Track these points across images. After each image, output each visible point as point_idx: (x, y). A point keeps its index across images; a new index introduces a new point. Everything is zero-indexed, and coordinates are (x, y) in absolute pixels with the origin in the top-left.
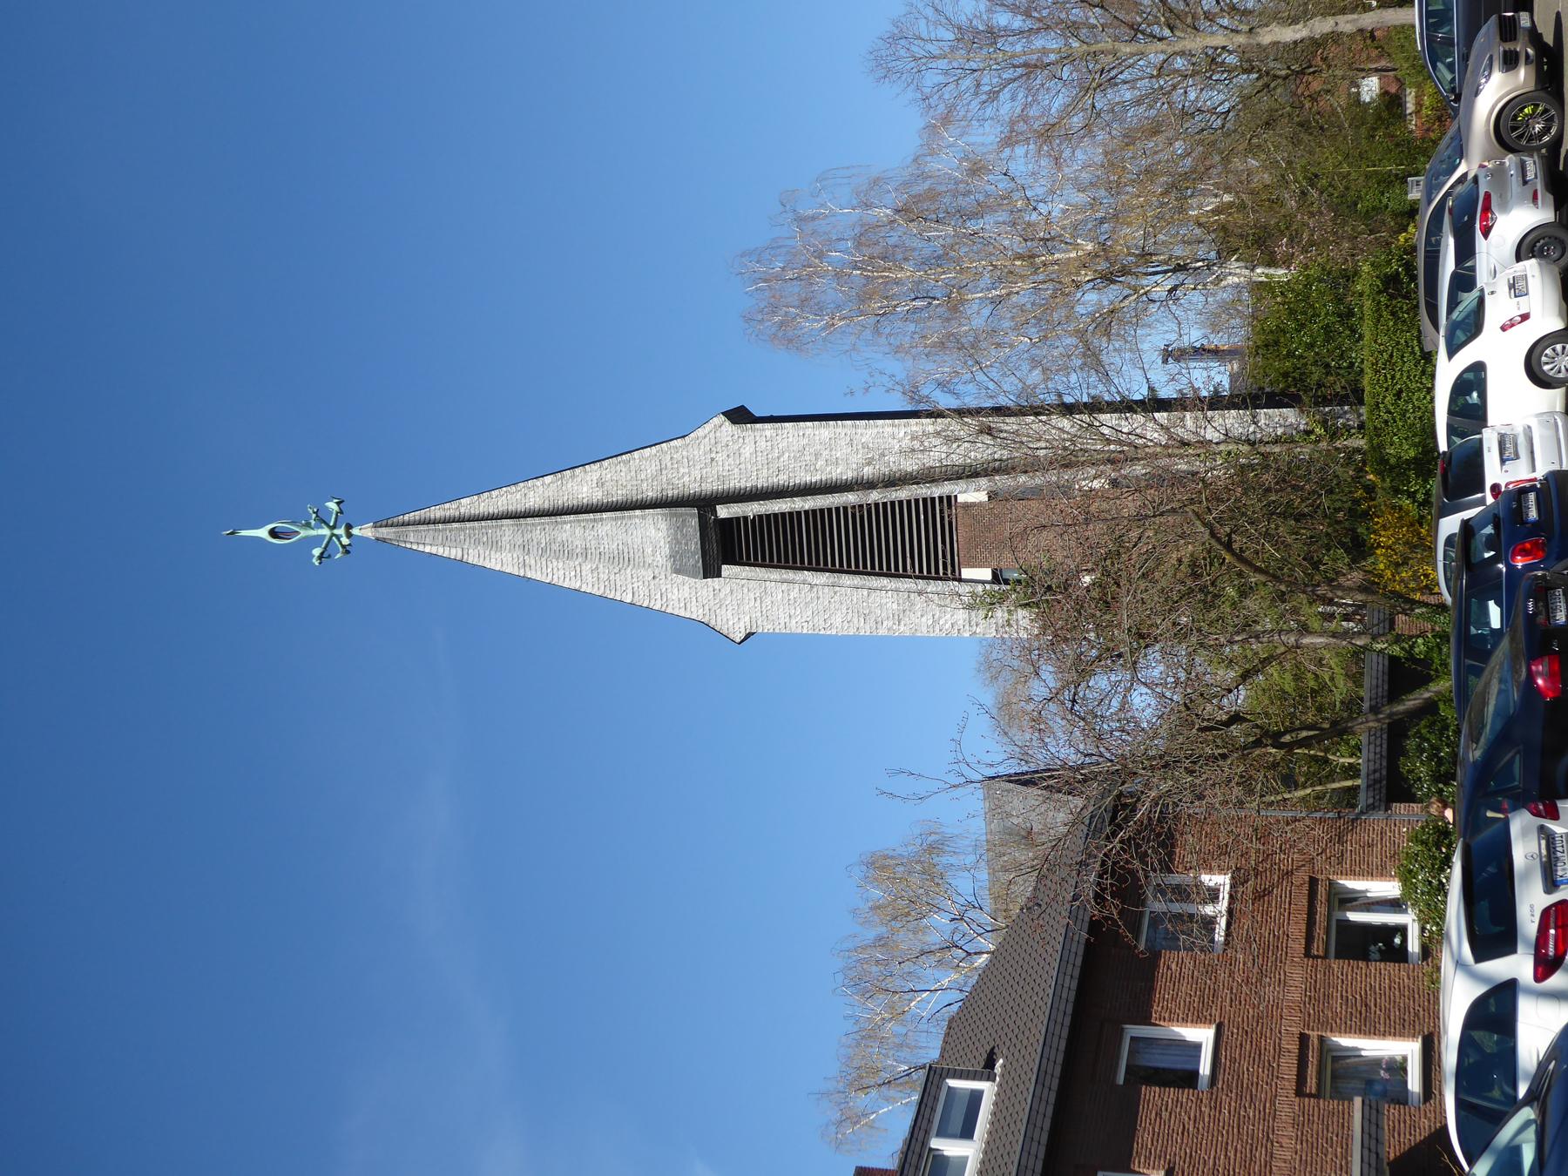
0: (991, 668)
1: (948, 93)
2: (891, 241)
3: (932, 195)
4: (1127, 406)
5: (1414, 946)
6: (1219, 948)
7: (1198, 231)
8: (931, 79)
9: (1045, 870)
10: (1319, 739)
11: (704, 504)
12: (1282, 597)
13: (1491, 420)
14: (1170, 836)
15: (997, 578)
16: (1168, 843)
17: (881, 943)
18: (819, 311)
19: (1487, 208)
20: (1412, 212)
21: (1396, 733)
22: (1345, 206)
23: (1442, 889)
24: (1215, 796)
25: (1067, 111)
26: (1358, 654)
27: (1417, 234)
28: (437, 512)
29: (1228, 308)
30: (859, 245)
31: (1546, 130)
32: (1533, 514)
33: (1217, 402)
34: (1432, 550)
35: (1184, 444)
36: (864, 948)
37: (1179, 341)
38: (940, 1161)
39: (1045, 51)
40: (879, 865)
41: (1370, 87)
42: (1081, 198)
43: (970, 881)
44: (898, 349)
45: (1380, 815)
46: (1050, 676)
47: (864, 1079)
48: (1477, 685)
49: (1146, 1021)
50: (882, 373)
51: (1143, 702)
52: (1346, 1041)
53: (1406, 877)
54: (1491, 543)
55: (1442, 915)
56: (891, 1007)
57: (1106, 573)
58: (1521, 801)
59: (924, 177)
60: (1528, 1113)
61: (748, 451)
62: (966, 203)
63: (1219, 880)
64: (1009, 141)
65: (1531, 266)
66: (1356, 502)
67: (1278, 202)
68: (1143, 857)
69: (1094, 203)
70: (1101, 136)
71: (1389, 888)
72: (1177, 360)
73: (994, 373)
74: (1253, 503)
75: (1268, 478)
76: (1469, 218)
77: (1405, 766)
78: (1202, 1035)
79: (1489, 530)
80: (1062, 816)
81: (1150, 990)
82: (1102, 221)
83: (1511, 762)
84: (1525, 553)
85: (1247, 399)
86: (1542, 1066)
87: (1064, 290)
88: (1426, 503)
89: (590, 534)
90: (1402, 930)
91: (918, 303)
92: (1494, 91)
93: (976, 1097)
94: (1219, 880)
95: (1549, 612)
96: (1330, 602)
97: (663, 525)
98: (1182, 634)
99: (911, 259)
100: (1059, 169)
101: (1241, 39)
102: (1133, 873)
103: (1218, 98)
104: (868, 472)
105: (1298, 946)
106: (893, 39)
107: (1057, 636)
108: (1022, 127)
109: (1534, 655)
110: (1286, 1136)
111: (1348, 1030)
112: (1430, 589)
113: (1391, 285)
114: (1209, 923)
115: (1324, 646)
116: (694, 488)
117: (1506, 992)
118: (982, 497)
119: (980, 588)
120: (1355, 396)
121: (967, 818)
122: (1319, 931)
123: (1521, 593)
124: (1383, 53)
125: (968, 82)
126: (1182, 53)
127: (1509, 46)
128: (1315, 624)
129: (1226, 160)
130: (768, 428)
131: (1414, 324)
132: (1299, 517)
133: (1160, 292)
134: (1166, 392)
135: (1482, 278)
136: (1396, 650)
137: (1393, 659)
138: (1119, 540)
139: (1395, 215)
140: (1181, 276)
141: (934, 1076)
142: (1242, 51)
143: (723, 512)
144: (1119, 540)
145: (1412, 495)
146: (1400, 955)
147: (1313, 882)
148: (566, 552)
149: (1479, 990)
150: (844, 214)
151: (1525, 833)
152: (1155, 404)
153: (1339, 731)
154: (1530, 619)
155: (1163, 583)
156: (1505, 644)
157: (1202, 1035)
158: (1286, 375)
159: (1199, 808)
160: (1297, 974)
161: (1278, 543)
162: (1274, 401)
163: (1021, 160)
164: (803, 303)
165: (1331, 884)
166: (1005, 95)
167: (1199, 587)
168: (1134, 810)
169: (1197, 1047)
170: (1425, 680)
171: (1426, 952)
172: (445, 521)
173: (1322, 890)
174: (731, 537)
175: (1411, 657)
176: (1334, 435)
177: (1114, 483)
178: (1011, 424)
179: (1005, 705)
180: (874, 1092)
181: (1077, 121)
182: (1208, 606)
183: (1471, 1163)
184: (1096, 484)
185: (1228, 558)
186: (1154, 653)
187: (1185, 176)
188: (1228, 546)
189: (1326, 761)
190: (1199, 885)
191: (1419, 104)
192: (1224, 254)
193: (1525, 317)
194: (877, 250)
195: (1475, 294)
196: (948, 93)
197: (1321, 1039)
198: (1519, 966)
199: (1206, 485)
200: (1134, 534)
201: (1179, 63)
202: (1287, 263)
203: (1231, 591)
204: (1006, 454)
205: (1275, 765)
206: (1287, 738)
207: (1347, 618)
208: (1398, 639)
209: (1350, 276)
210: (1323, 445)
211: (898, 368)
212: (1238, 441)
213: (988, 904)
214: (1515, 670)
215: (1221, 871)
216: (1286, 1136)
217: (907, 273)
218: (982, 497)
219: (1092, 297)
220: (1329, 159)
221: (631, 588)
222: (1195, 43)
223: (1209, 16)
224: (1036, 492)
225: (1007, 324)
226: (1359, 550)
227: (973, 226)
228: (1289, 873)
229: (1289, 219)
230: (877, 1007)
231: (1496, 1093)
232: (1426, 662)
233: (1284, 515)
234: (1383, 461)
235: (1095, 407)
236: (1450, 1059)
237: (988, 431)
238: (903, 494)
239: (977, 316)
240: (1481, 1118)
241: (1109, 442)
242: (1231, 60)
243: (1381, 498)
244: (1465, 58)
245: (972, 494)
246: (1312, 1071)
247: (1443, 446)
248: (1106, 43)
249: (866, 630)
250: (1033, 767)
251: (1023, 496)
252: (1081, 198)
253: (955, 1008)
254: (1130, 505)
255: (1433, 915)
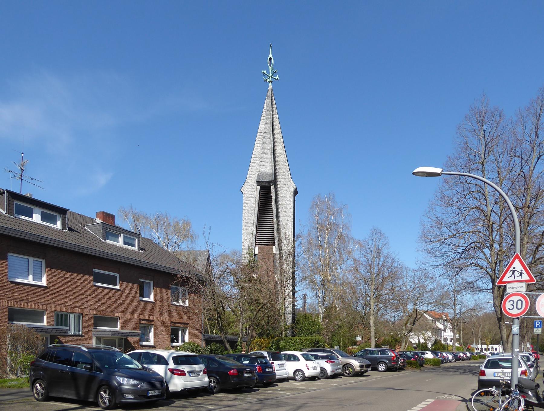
0: (234, 253)
1: (367, 246)
2: (334, 232)
3: (344, 242)
4: (294, 286)
5: (174, 344)
6: (172, 303)
7: (331, 302)
8: (370, 242)
9: (188, 264)
10: (219, 326)
11: (275, 182)
12: (250, 319)
13: (287, 362)
14: (197, 293)
15: (255, 255)
16: (195, 293)
17: (169, 224)
18: (320, 214)
19: (331, 362)
20: (332, 347)
21: (221, 342)
22: (334, 333)
23: (187, 350)
24: (206, 303)
25: (360, 273)
26: (238, 335)
27: (327, 348)
28: (275, 108)
29: (314, 308)
30: (334, 224)
31: (347, 373)
32: (267, 370)
33: (294, 306)
34: (260, 350)
35: (285, 299)
36: (167, 219)
37: (307, 298)
38: (118, 236)
39: (374, 269)
40: (187, 224)
41: (359, 339)
42: (340, 277)
43: (185, 246)
44: (309, 233)
45: (203, 338)
46: (233, 267)
47: (136, 219)
48: (231, 359)
49: (154, 286)
50: (304, 229)
51: (227, 288)
52: (153, 330)
53: (189, 343)
54: (261, 362)
55: (182, 350)
56: (154, 226)
57: (256, 280)
58: (207, 367)
59: (349, 240)
60: (140, 366)
61: (287, 194)
62: (342, 250)
63: (187, 304)
64: (355, 260)
65: (319, 370)
66: (271, 335)
67: (336, 319)
68: (192, 287)
69: (339, 279)
70: (354, 281)
71: (187, 340)
72: (303, 297)
73: (302, 255)
74: (271, 313)
75: (277, 316)
76: (330, 358)
77: (214, 344)
78: (152, 299)
79: (264, 361)
80: (200, 268)
81: (162, 288)
82: (335, 281)
83: (214, 365)
84: (259, 369)
85: (294, 313)
86: (151, 370)
87: (320, 272)
88: (270, 349)
89: (268, 151)
90: (178, 342)
91: (320, 238)
92: (356, 363)
93: (134, 246)
94: (187, 304)
95: (246, 373)
96: (249, 329)
97: (270, 171)
98: (242, 297)
99: (330, 235)
100: (348, 271)
101: (372, 312)
102: (188, 284)
103: (360, 306)
104: (281, 224)
105: (173, 320)
106: (380, 234)
107: (242, 269)
108: (358, 263)
109: (237, 370)
110: (131, 316)
111: (155, 330)
112: (252, 349)
113: (317, 343)
114: (177, 301)
115: (240, 328)
116: (279, 180)
117: (166, 363)
118: (274, 252)
119: (253, 251)
120: (294, 335)
121: (200, 246)
122: (177, 325)
123: (251, 368)
124: (366, 341)
125: (369, 251)
126: (370, 299)
127: (364, 366)
128: (244, 326)
129: (346, 308)
130: (292, 200)
131: (308, 347)
132: (268, 323)
133: (319, 294)
134: (296, 294)
135: (317, 361)
136: (239, 342)
137: (237, 342)
138: (264, 283)
139: (331, 344)
140: (322, 298)
141: (138, 236)
142: (369, 312)
143: (273, 187)
144: (264, 283)
145: (272, 346)
146: (172, 341)
147: (188, 324)
148: (264, 144)
149: (166, 358)
150: (342, 220)
151: (200, 367)
152: (294, 292)
153: (221, 330)
154: (245, 369)
155: (254, 293)
156: (240, 364)
157: (152, 299)
158: (299, 320)
159: (203, 300)
160: (167, 320)
161: (262, 319)
162: (293, 318)
163: (350, 263)
164: (321, 209)
165: (187, 328)
166: (365, 260)
167: (253, 301)
168: (202, 285)
169: (149, 297)
170: (232, 348)
171: (173, 347)
172: (272, 110)
173: (185, 326)
174: (266, 187)
175: (237, 346)
176: (285, 330)
177: (277, 283)
178: (291, 259)
179: (226, 256)
180: (133, 220)
181: (358, 276)
182: (249, 303)
183: (128, 355)
184: (276, 279)
185: (259, 308)
186: (238, 291)
187: (343, 300)
188: (262, 308)
189: (214, 327)
190: (186, 299)
191: (354, 348)
192: (326, 308)
193: (308, 369)
194: (332, 228)
195: (314, 359)
196: (367, 246)
197: (153, 325)
198: (172, 365)
199: (275, 303)
200: (265, 287)
201: (368, 299)
202: (323, 321)
203: (252, 308)
204: (284, 258)
205: (213, 316)
206: (219, 319)
207: (246, 332)
208: (241, 343)
209: (319, 334)
210: (283, 328)
211: (305, 233)
212: (285, 310)
213: (179, 250)
214: (234, 366)
215: (189, 304)
216: (131, 316)
217: (327, 236)
218: (274, 252)
219: (319, 279)
220: (344, 330)
221: (255, 161)
222: (372, 302)
223: (377, 305)
224: (275, 265)
225: (314, 259)
226: (260, 335)
227: (336, 251)
228: (189, 319)
229: (332, 321)
230: (153, 222)
231: (144, 360)
232: (236, 348)
233: (268, 320)
234: (279, 341)
235: (294, 279)
236: (151, 351)
237: (289, 254)
238: (276, 233)
239: (316, 252)
240: (138, 357)
241: (286, 282)
242: (368, 310)
243: (272, 340)
244: (363, 358)
245: (275, 249)
246: (146, 322)
247: (282, 353)
248: (374, 283)
249: (244, 223)
250: (212, 262)
251: (274, 262)
252: (340, 277)
253: (154, 241)
254: (272, 286)
255: (181, 348)
